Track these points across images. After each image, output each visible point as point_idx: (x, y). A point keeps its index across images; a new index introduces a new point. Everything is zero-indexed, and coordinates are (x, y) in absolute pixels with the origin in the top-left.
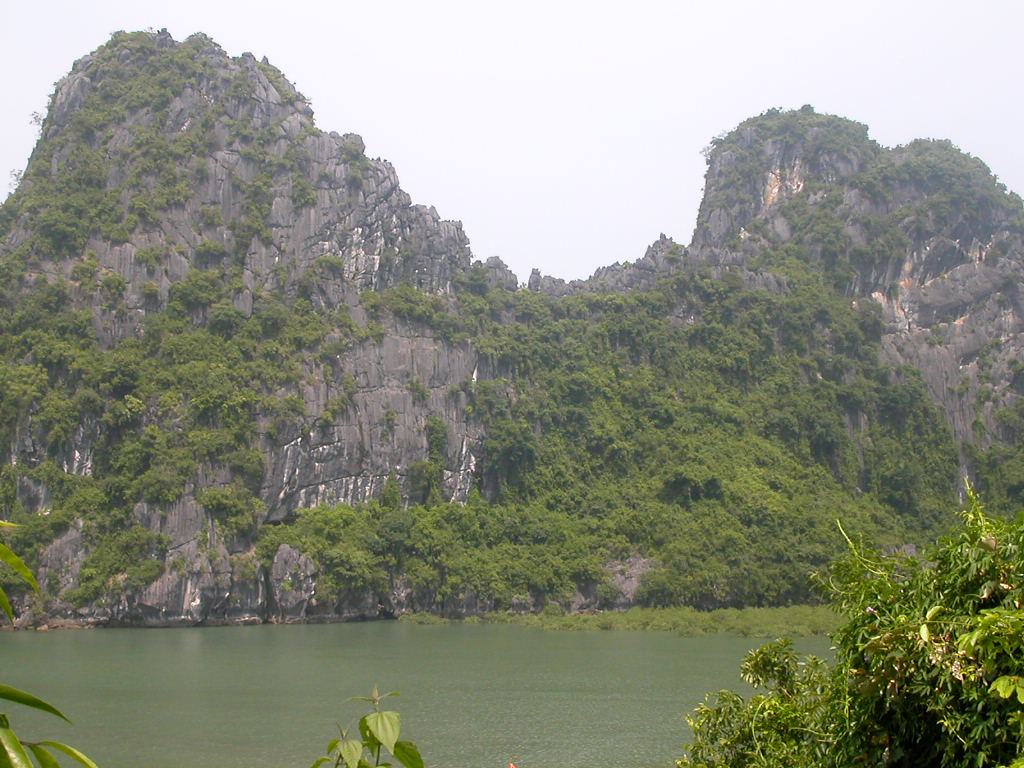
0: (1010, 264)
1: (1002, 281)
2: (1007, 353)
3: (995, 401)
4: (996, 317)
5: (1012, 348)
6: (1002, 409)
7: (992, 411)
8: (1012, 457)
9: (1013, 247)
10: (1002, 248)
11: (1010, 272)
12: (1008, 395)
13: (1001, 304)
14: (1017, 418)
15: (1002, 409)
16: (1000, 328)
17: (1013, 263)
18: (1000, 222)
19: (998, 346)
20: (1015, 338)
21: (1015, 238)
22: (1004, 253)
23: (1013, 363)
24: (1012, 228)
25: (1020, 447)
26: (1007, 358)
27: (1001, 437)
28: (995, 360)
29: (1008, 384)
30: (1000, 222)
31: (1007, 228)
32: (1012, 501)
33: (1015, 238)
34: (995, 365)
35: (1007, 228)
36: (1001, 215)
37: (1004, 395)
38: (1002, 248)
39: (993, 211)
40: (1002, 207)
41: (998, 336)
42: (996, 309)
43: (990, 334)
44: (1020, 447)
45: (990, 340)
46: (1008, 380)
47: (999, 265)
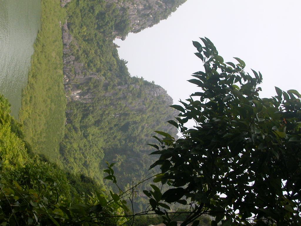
0: (156, 8)
1: (151, 6)
2: (131, 7)
3: (118, 3)
4: (142, 4)
5: (133, 8)
6: (115, 5)
7: (115, 2)
8: (102, 7)
9: (161, 9)
10: (161, 6)
11: (154, 8)
12: (119, 6)
13: (145, 5)
14: (113, 9)
15: (115, 5)
16: (138, 5)
17: (157, 9)
18: (168, 6)
19: (133, 4)
20: (135, 8)
21: (163, 10)
22: (159, 7)
23: (128, 8)
24: (166, 9)
25: (105, 9)
26: (130, 6)
27: (108, 4)
28: (129, 3)
29: (123, 6)
30: (168, 6)
31: (166, 8)
32: (89, 7)
33: (163, 10)
34: (128, 3)
35: (166, 8)
36: (170, 6)
37: (119, 5)
38: (161, 6)
39: (171, 4)
40: (172, 7)
41: (136, 4)
42: (143, 4)
43: (137, 2)
44: (105, 9)
45: (135, 2)
46: (124, 6)
47: (156, 5)
